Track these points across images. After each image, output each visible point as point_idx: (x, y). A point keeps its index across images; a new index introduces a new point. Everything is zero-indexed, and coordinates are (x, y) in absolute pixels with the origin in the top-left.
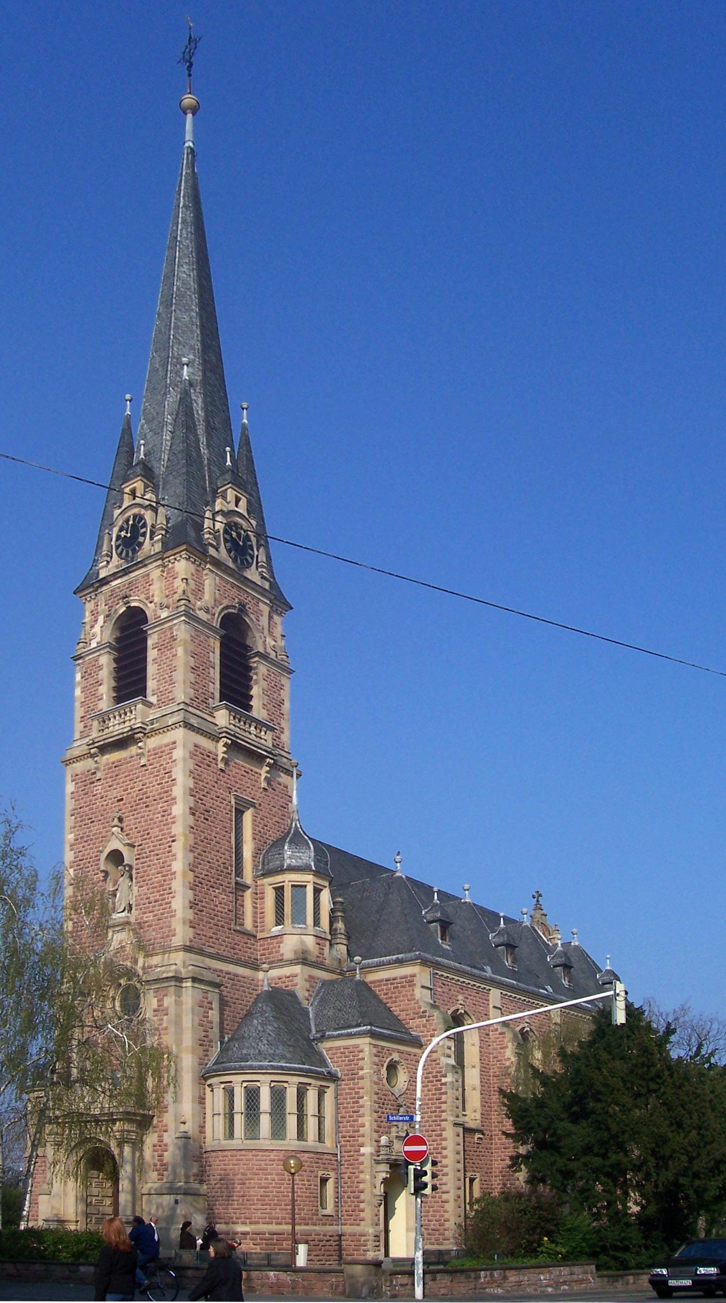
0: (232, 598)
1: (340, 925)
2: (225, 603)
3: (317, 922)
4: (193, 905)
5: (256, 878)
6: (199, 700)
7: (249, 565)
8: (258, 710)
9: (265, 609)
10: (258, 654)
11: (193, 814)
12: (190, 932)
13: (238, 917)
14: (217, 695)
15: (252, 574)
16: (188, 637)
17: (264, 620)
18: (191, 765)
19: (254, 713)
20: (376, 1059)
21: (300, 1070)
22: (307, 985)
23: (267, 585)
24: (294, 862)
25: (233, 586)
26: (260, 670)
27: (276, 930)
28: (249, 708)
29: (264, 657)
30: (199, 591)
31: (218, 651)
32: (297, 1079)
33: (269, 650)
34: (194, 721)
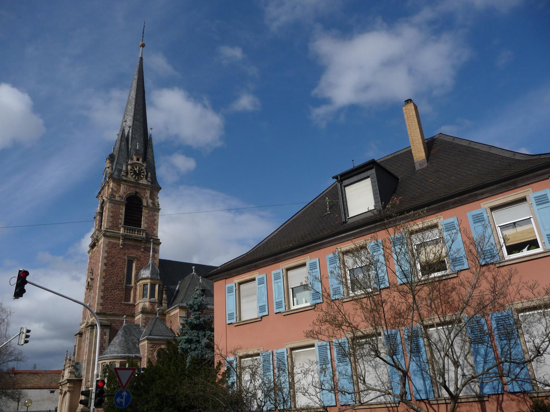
0: (132, 191)
1: (164, 296)
2: (128, 193)
3: (152, 295)
4: (102, 298)
5: (135, 284)
6: (114, 225)
7: (142, 179)
8: (144, 225)
9: (149, 192)
10: (145, 206)
11: (106, 265)
12: (101, 308)
13: (127, 298)
14: (123, 223)
15: (144, 181)
16: (110, 207)
17: (148, 195)
18: (106, 249)
19: (142, 227)
20: (151, 349)
21: (121, 356)
22: (145, 321)
23: (149, 184)
24: (144, 276)
25: (133, 187)
26: (145, 212)
27: (138, 302)
28: (140, 225)
29: (147, 206)
30: (119, 190)
31: (124, 209)
32: (119, 360)
33: (149, 204)
34: (108, 234)
